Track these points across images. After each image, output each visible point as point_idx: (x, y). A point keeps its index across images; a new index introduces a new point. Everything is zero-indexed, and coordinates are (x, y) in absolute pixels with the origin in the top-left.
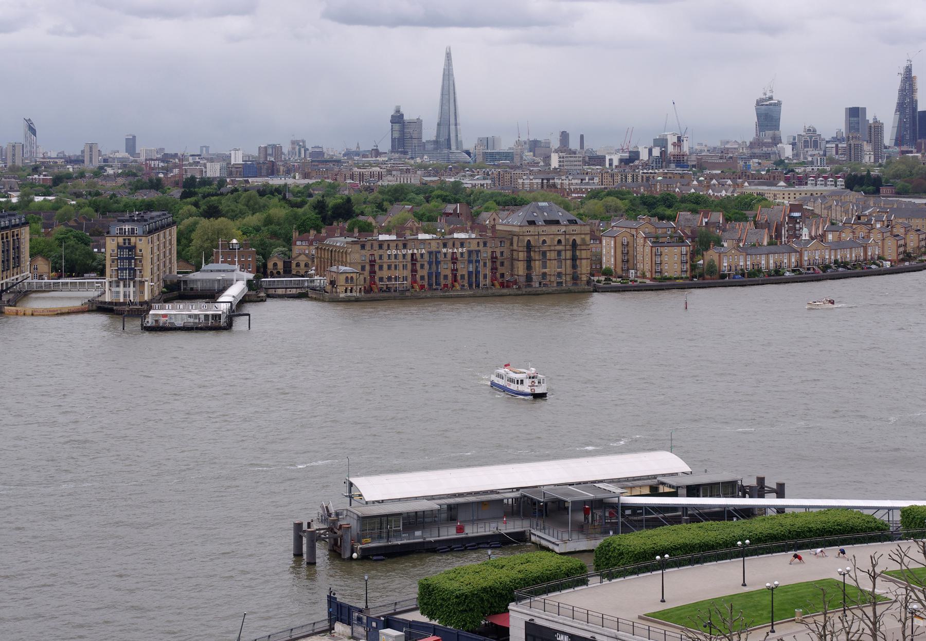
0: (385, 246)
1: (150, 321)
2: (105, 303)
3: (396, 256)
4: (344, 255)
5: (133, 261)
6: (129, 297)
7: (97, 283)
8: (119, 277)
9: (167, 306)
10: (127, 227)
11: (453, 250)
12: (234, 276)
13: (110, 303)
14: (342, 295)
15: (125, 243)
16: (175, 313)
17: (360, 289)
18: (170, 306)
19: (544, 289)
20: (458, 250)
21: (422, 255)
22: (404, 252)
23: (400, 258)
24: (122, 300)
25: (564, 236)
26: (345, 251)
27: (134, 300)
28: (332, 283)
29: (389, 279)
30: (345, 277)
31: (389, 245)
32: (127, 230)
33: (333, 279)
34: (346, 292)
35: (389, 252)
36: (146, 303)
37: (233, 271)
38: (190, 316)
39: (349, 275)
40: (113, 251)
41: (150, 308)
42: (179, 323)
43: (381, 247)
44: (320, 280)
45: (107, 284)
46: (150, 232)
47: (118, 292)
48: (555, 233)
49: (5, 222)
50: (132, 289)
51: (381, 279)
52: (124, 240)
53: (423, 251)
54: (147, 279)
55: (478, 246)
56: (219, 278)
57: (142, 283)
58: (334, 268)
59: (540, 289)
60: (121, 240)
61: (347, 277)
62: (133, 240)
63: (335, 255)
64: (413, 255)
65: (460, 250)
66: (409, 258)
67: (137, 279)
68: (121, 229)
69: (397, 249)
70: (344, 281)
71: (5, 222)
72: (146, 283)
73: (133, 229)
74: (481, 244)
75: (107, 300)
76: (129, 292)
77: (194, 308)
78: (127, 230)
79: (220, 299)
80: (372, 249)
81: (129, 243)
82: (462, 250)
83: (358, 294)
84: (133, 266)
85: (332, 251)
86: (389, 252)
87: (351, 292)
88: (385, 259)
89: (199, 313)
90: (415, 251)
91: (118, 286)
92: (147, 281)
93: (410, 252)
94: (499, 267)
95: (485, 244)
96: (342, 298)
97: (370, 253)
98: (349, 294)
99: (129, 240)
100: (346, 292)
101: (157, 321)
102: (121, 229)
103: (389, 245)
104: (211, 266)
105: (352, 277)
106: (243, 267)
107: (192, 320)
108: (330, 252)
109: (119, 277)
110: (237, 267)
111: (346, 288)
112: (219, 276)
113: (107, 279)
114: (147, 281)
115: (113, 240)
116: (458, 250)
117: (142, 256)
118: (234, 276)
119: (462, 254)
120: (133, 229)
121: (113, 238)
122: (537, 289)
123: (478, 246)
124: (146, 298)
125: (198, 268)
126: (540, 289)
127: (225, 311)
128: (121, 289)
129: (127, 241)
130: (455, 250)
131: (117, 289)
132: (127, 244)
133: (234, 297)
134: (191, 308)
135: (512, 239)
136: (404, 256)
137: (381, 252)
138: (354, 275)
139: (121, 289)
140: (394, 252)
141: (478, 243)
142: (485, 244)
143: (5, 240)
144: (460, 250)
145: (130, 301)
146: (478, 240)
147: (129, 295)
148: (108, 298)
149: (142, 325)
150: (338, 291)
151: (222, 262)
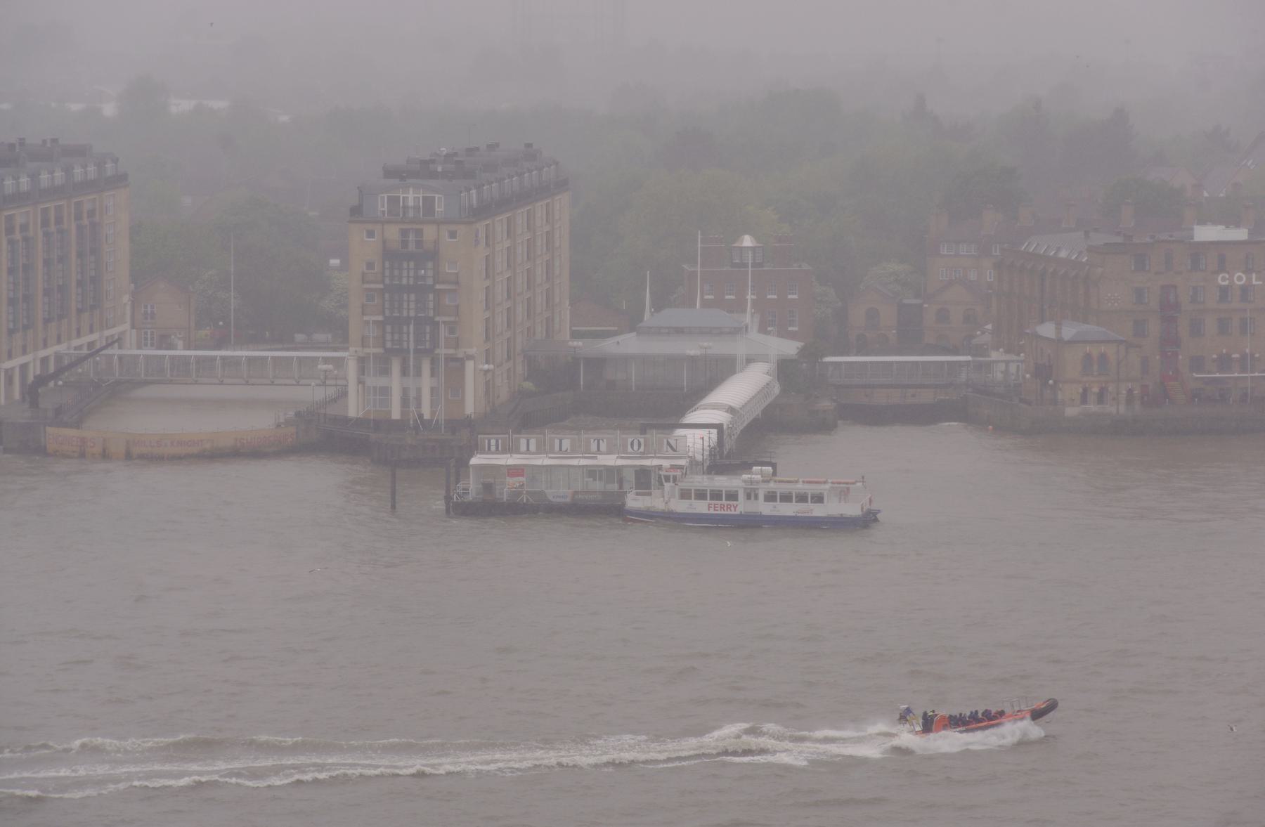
1: (472, 487)
2: (346, 420)
3: (1245, 290)
5: (431, 297)
6: (419, 405)
7: (326, 360)
8: (389, 345)
9: (523, 442)
10: (411, 197)
12: (739, 348)
13: (359, 422)
14: (1071, 412)
15: (405, 244)
16: (547, 462)
17: (1130, 391)
18: (533, 442)
24: (396, 415)
27: (433, 413)
28: (1043, 372)
29: (1224, 362)
32: (411, 203)
34: (1084, 399)
35: (1222, 280)
36: (468, 423)
37: (736, 331)
38: (592, 472)
40: (370, 265)
41: (474, 448)
42: (559, 492)
44: (1007, 363)
45: (352, 369)
46: (483, 211)
47: (385, 391)
49: (52, 172)
50: (426, 382)
51: (1197, 363)
52: (404, 233)
54: (472, 351)
56: (692, 353)
57: (456, 366)
58: (1047, 330)
60: (393, 232)
61: (1088, 356)
62: (429, 232)
67: (442, 351)
68: (394, 201)
69: (1248, 271)
71: (52, 172)
72: (470, 365)
73: (429, 203)
75: (352, 412)
76: (419, 390)
77: (603, 447)
78: (411, 203)
79: (692, 418)
81: (419, 243)
83: (1122, 409)
84: (431, 314)
86: (1222, 280)
87: (1101, 398)
89: (620, 462)
91: (386, 372)
92: (470, 357)
98: (1093, 407)
99: (419, 233)
100: (1084, 399)
101: (488, 487)
102: (394, 201)
104: (673, 316)
105: (1103, 357)
106: (772, 321)
107: (597, 486)
109: (389, 345)
110: (749, 318)
111: (1085, 391)
112: (692, 348)
113: (352, 349)
114: (470, 357)
115: (371, 234)
117: (457, 283)
118: (739, 348)
120: (429, 203)
121: (370, 227)
124: (470, 409)
125: (632, 323)
127: (699, 457)
128: (395, 383)
129: (411, 237)
131: (381, 382)
132: (412, 247)
133: (731, 410)
134: (594, 447)
139: (395, 383)
140: (1240, 279)
143: (53, 228)
145: (421, 416)
147: (418, 399)
148: (353, 408)
149: (448, 498)
150: (1060, 396)
151: (705, 304)
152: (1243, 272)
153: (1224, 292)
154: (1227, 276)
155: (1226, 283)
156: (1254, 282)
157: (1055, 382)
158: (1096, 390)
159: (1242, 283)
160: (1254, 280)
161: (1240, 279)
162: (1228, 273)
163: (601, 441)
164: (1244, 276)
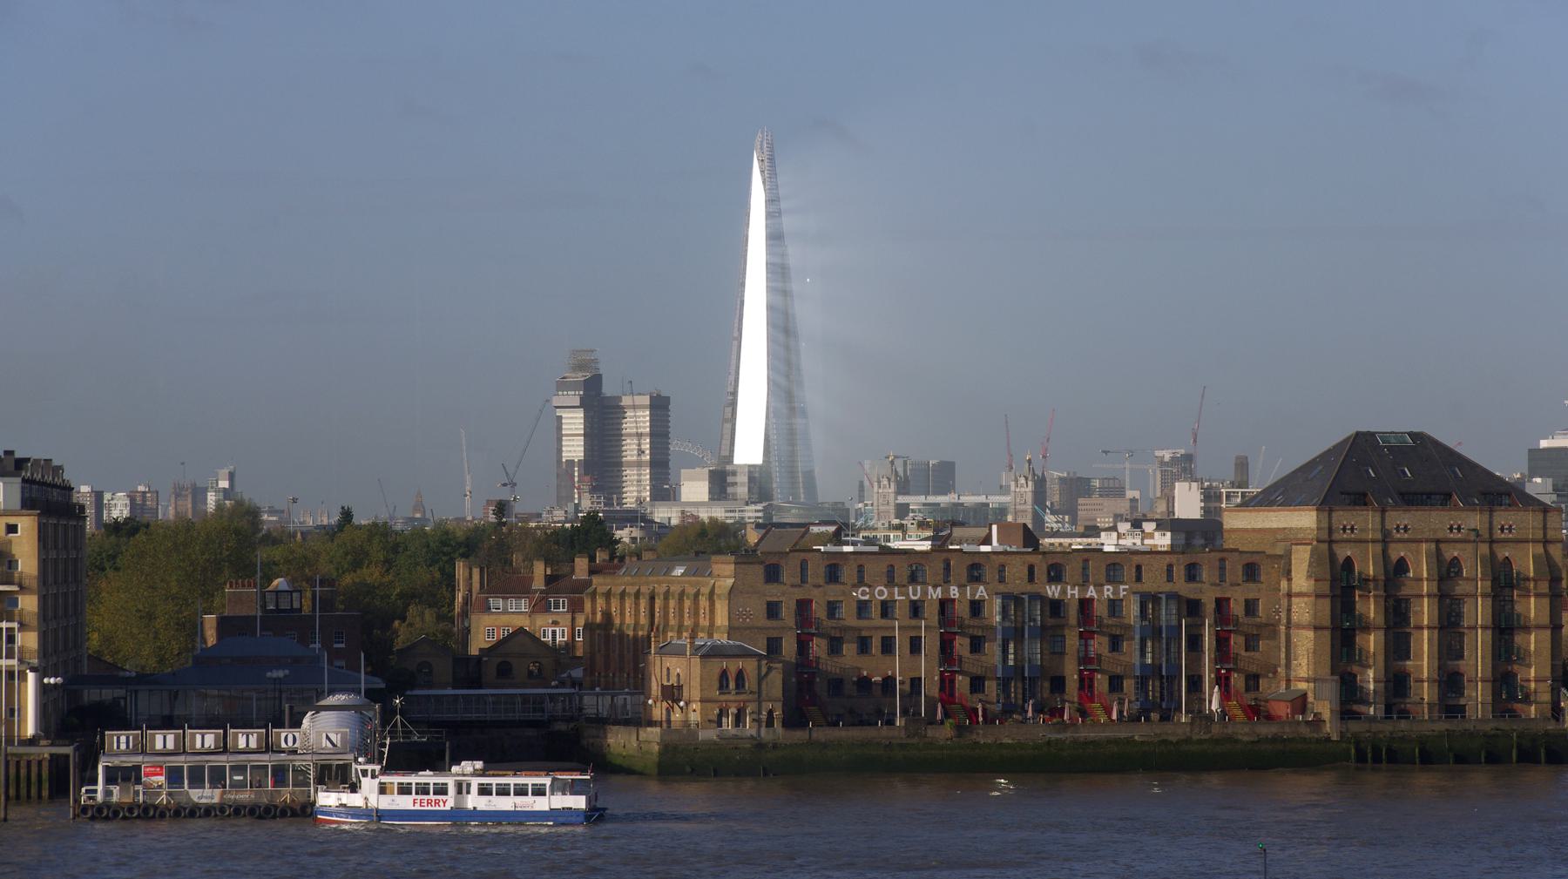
0: (848, 573)
3: (886, 608)
4: (704, 602)
11: (1084, 584)
17: (770, 713)
19: (1403, 725)
20: (1100, 592)
21: (976, 607)
22: (914, 593)
23: (901, 613)
25: (1470, 547)
26: (705, 590)
30: (716, 672)
31: (861, 569)
33: (673, 681)
35: (860, 594)
39: (733, 666)
43: (833, 575)
48: (1440, 535)
53: (981, 592)
55: (1170, 578)
59: (1388, 727)
61: (724, 675)
63: (666, 607)
64: (945, 604)
65: (1108, 591)
66: (931, 613)
69: (890, 582)
70: (716, 685)
74: (1179, 573)
80: (804, 581)
82: (1116, 592)
85: (652, 599)
87: (739, 719)
88: (848, 616)
90: (954, 592)
93: (936, 594)
94: (1243, 653)
95: (1192, 573)
96: (705, 742)
97: (799, 594)
103: (861, 569)
105: (740, 675)
108: (643, 603)
116: (1100, 592)
119: (1114, 605)
122: (1375, 727)
123: (1170, 578)
126: (1388, 727)
130: (1091, 592)
135: (1287, 557)
136: (916, 609)
137: (833, 592)
138: (750, 666)
140: (882, 593)
141: (1170, 566)
142: (1192, 573)
144: (1108, 591)
146: (1168, 559)
152: (886, 586)
153: (862, 607)
154: (867, 590)
155: (867, 598)
156: (897, 598)
157: (687, 704)
158: (732, 710)
159: (882, 598)
160: (896, 595)
161: (881, 593)
162: (869, 586)
163: (250, 736)
164: (885, 590)
